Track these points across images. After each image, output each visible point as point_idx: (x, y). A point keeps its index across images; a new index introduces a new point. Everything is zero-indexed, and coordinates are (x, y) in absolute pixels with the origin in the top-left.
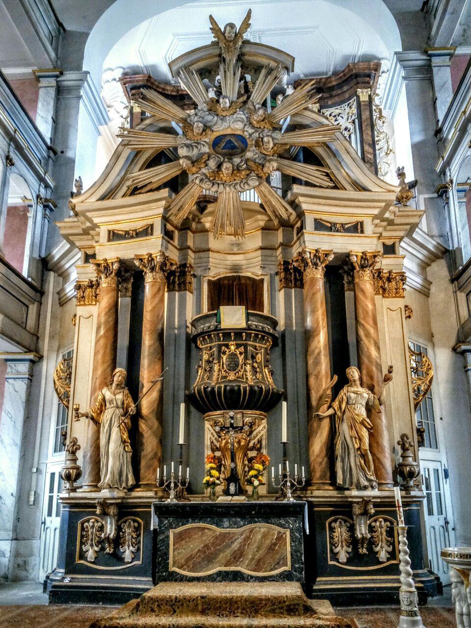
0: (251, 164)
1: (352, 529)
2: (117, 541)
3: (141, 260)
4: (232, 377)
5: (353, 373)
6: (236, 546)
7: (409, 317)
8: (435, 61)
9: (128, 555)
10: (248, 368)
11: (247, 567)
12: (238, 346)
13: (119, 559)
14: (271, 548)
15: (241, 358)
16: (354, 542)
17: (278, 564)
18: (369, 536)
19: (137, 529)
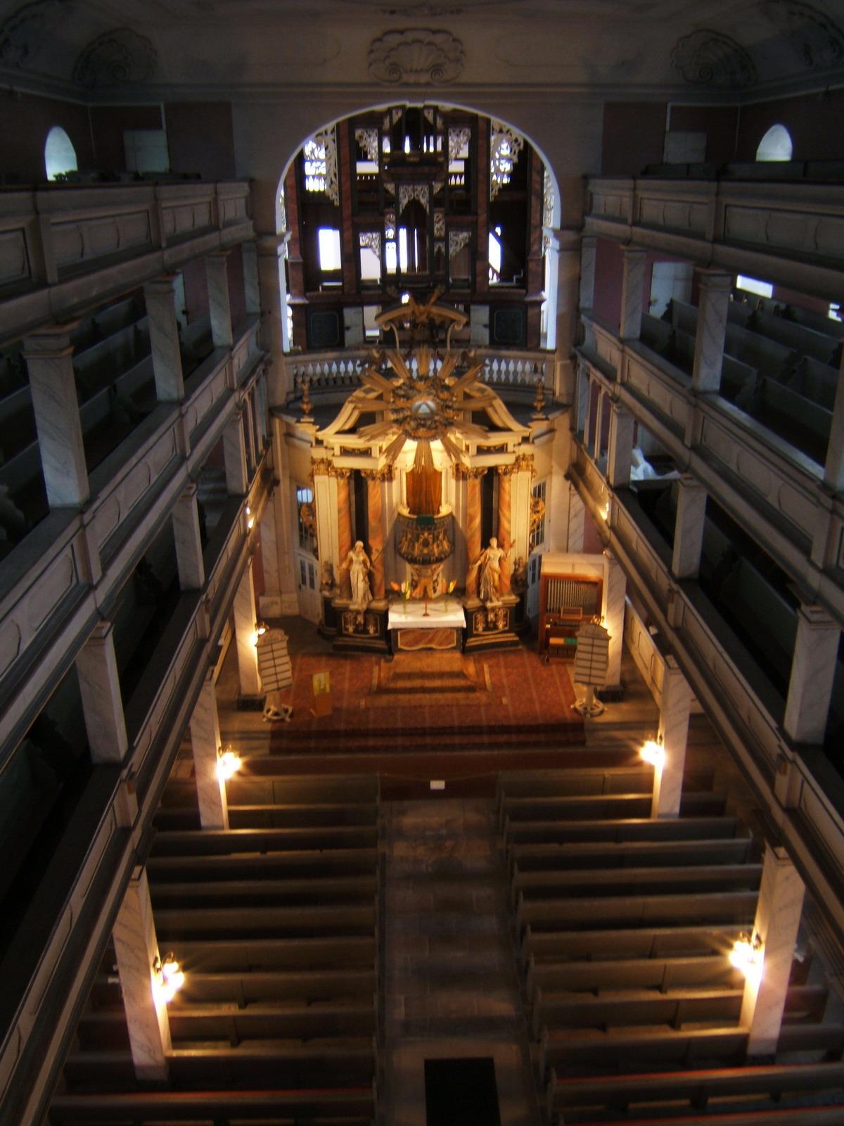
0: (438, 424)
1: (486, 616)
2: (365, 624)
3: (365, 473)
4: (426, 551)
5: (494, 542)
6: (430, 636)
7: (535, 476)
8: (585, 240)
9: (372, 630)
10: (435, 546)
11: (436, 645)
12: (429, 534)
13: (367, 632)
14: (447, 638)
15: (431, 541)
16: (486, 622)
17: (450, 643)
18: (494, 620)
19: (376, 619)
